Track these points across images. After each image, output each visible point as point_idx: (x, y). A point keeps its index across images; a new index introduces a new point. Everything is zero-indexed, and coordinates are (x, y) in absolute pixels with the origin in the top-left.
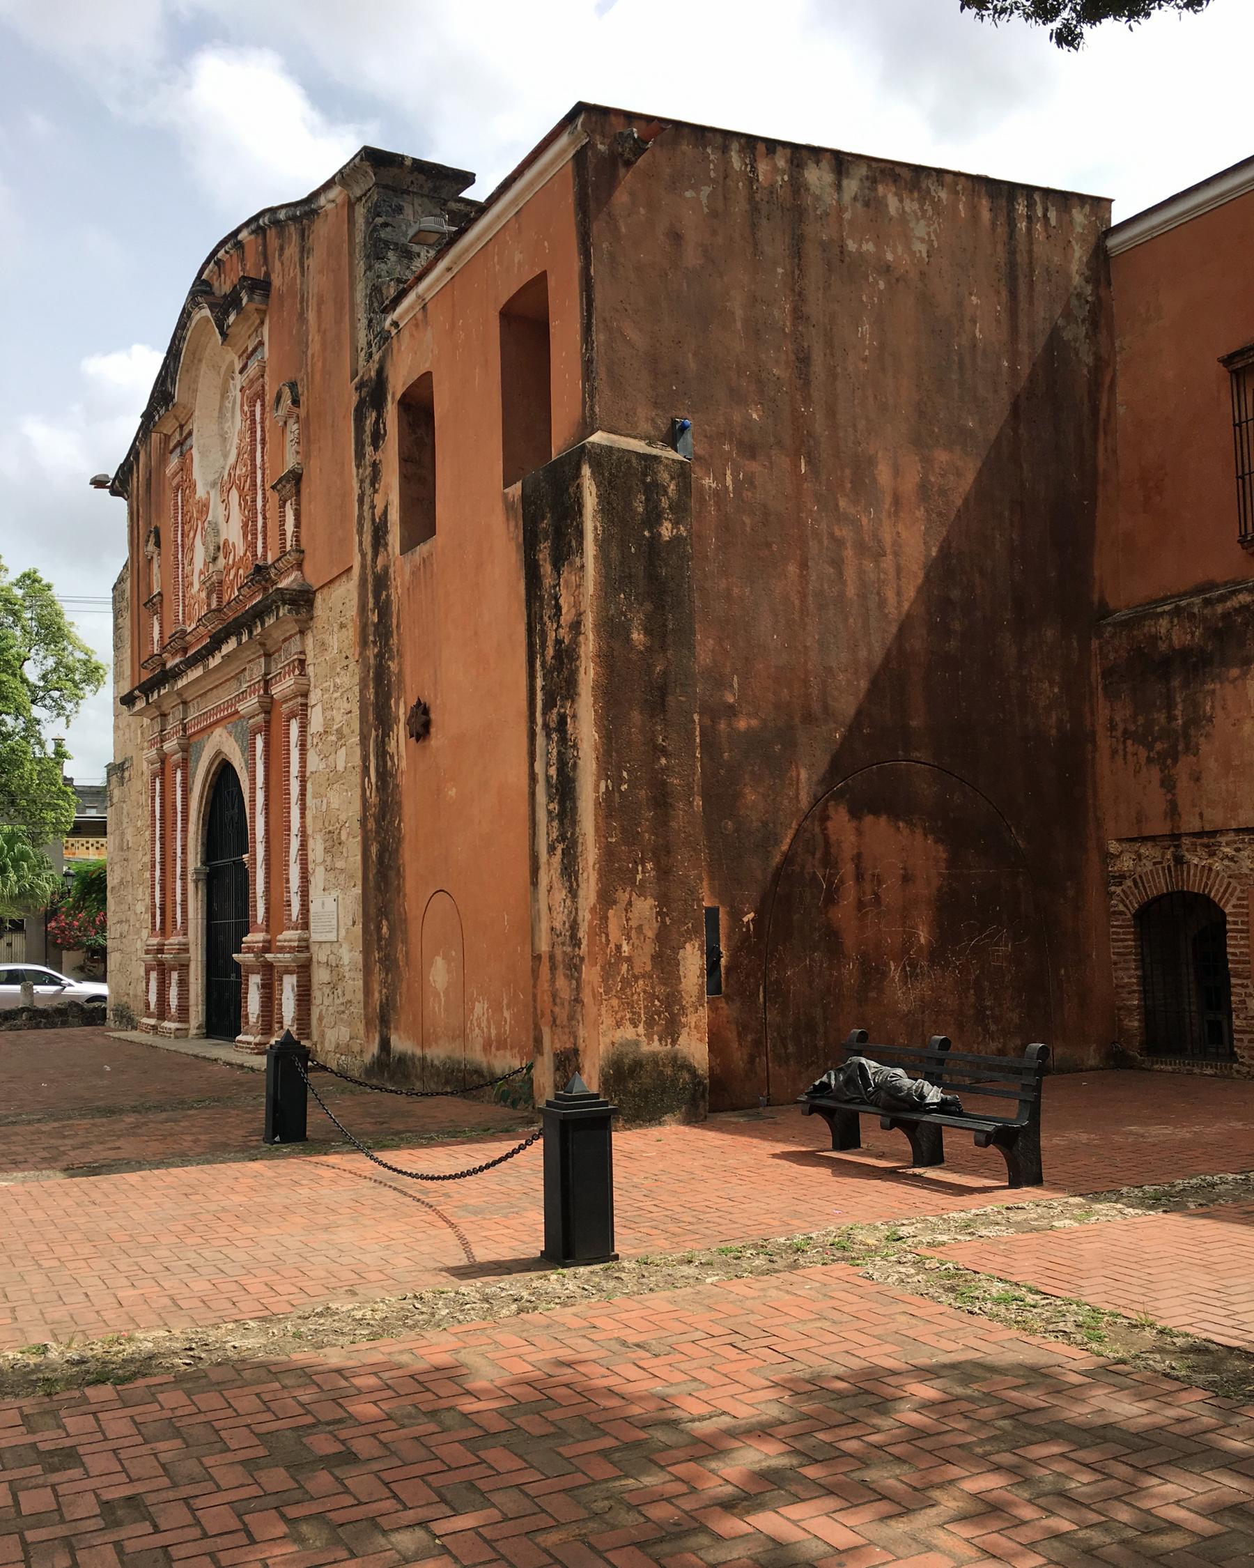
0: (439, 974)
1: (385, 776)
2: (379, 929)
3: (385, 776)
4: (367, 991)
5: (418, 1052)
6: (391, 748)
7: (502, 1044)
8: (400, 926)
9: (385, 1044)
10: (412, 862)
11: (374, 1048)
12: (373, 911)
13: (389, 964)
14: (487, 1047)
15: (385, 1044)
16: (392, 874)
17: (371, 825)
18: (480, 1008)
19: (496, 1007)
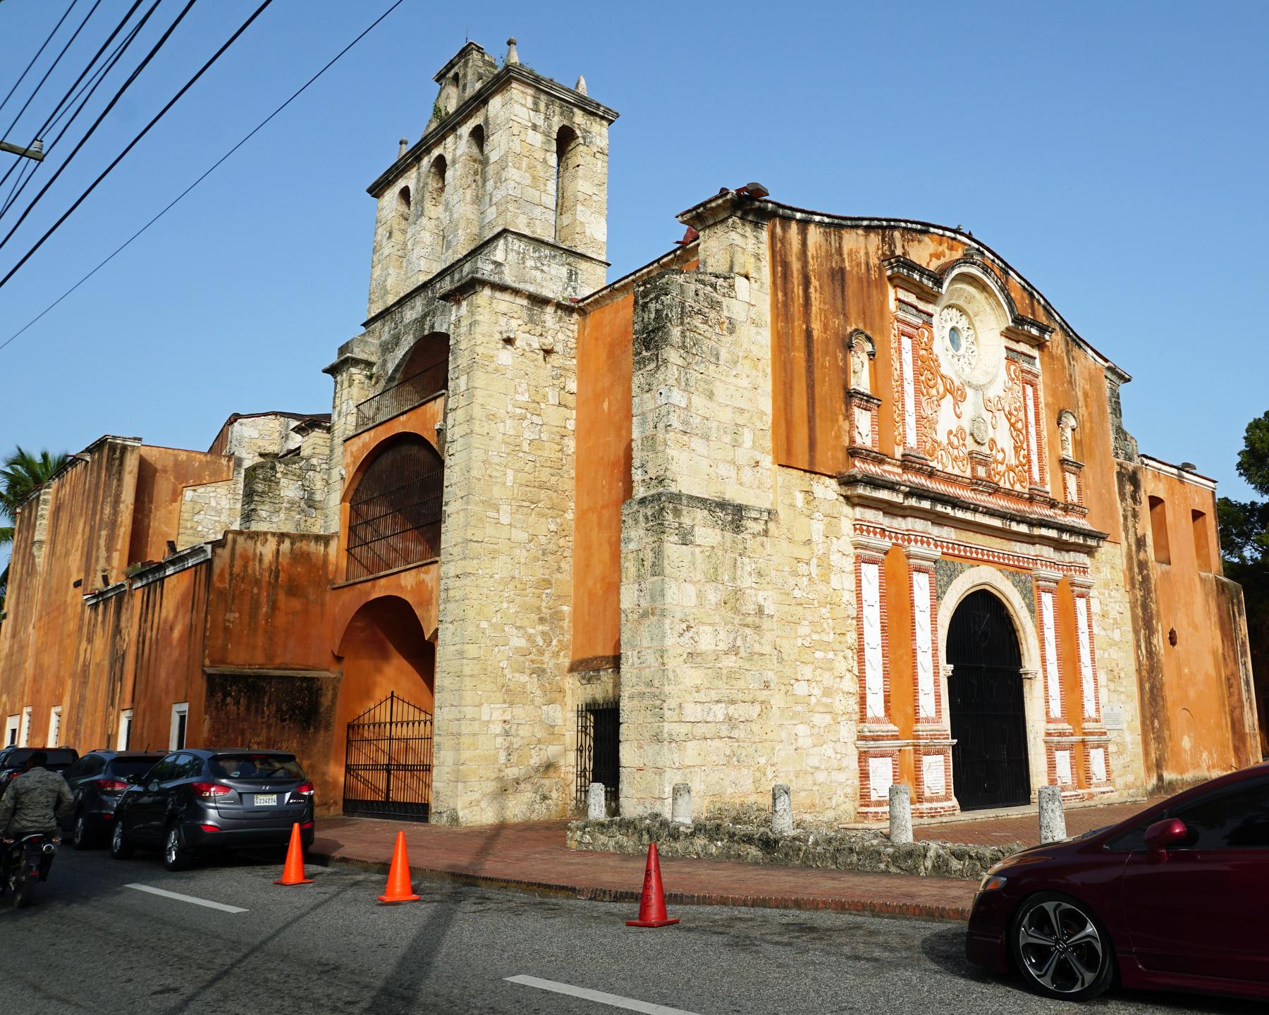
0: (1186, 743)
1: (1151, 654)
2: (1152, 723)
3: (1151, 654)
4: (1147, 753)
5: (1179, 777)
6: (1155, 641)
7: (1214, 767)
8: (1165, 723)
9: (1160, 778)
10: (1171, 694)
11: (1154, 781)
12: (1148, 715)
13: (1159, 739)
14: (1208, 769)
15: (1160, 778)
16: (1159, 699)
17: (1144, 673)
18: (1205, 755)
19: (1210, 754)
